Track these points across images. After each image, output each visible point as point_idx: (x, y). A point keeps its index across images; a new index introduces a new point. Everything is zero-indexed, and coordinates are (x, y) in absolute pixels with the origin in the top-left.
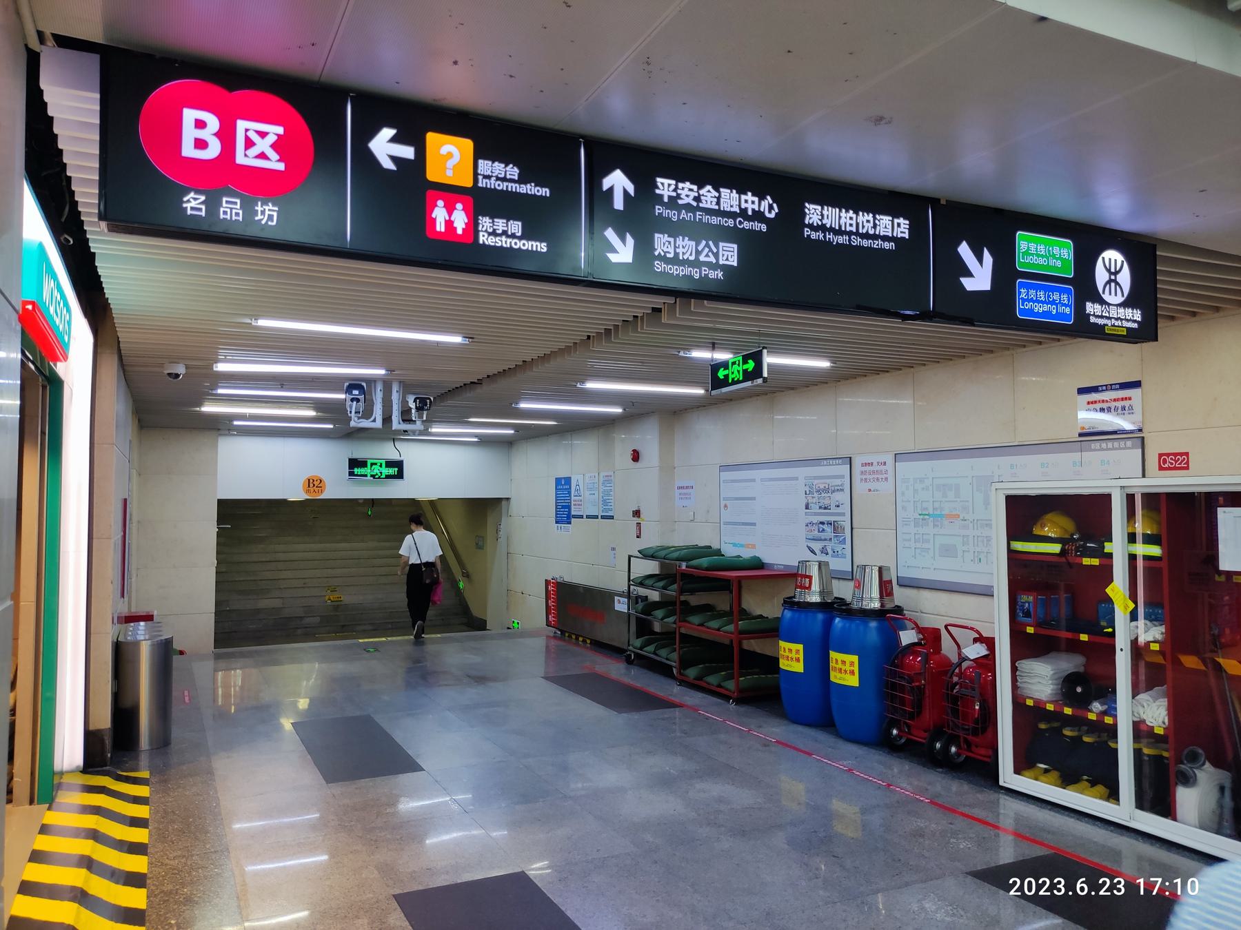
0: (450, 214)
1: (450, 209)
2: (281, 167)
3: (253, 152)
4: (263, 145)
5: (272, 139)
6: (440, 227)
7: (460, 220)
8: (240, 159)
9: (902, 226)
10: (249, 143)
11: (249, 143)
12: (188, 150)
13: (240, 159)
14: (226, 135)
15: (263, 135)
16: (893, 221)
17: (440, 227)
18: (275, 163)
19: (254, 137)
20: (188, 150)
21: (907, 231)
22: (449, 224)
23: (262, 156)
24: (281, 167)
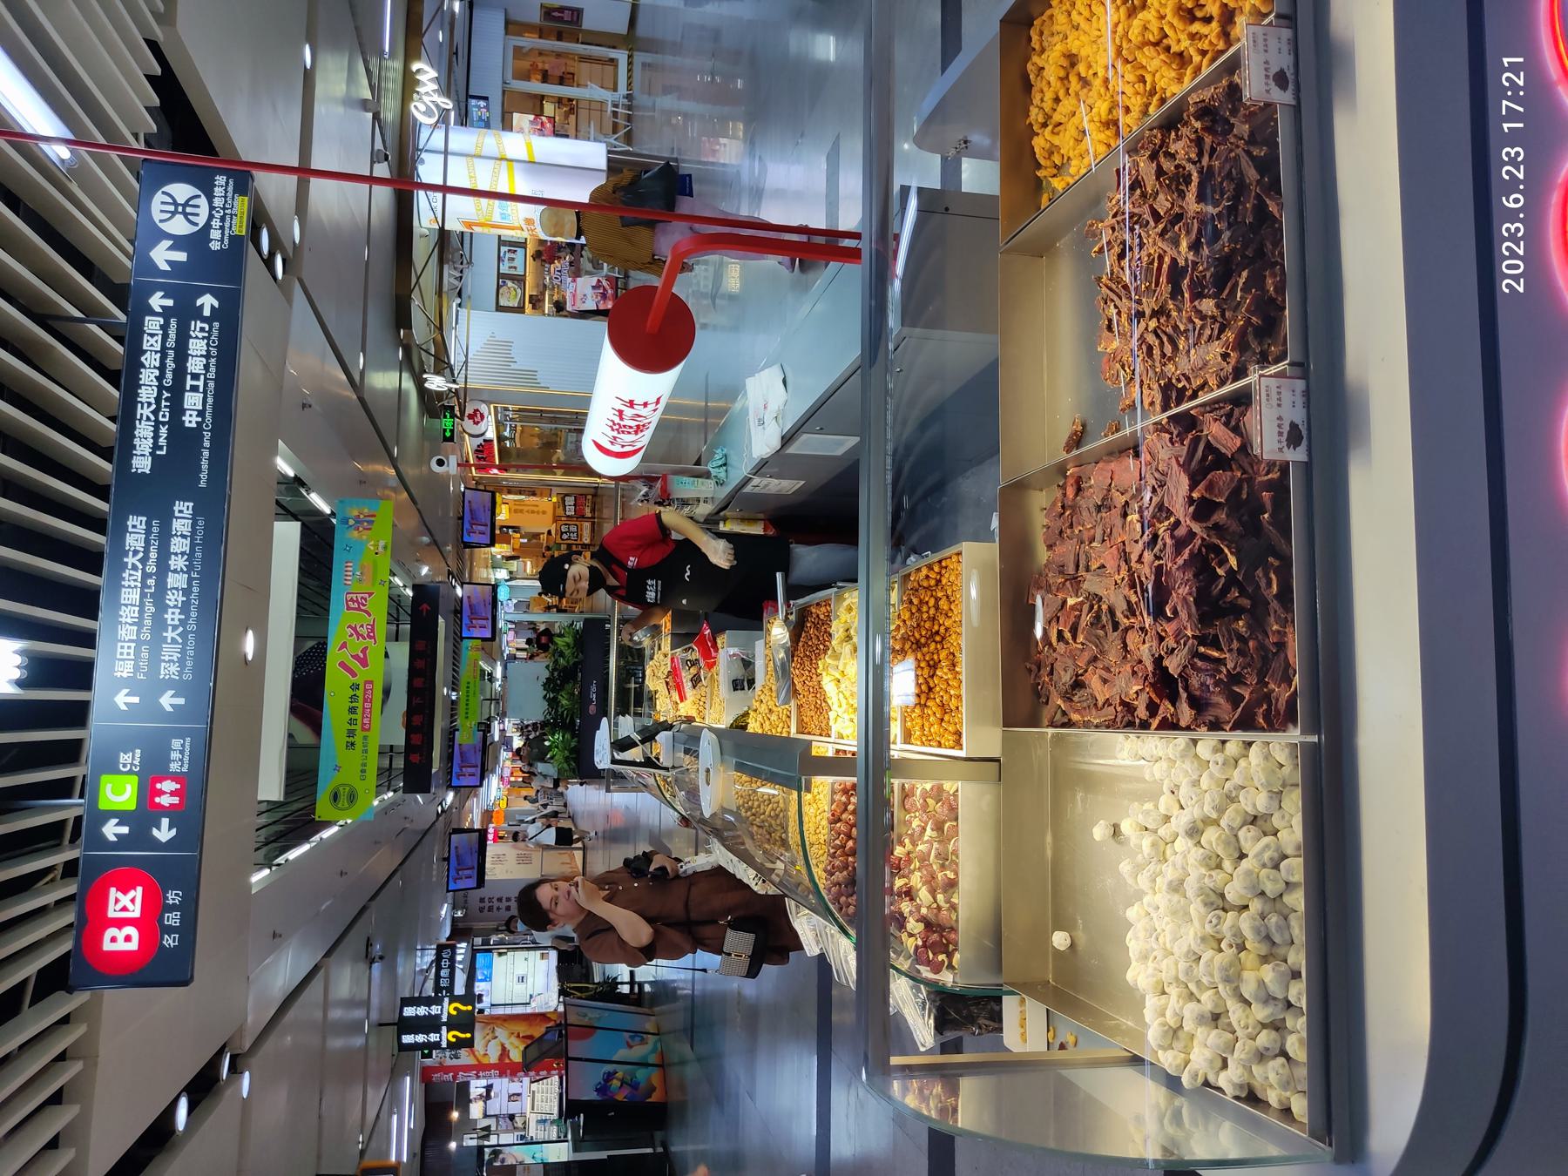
0: (164, 793)
1: (161, 793)
2: (140, 889)
3: (130, 906)
4: (125, 900)
5: (120, 895)
6: (176, 800)
7: (168, 786)
8: (137, 914)
9: (134, 523)
10: (124, 909)
11: (124, 909)
12: (133, 946)
13: (137, 914)
14: (120, 923)
15: (117, 901)
16: (130, 533)
17: (176, 800)
18: (138, 893)
19: (120, 906)
20: (133, 946)
21: (140, 518)
22: (172, 794)
23: (133, 901)
24: (140, 889)
